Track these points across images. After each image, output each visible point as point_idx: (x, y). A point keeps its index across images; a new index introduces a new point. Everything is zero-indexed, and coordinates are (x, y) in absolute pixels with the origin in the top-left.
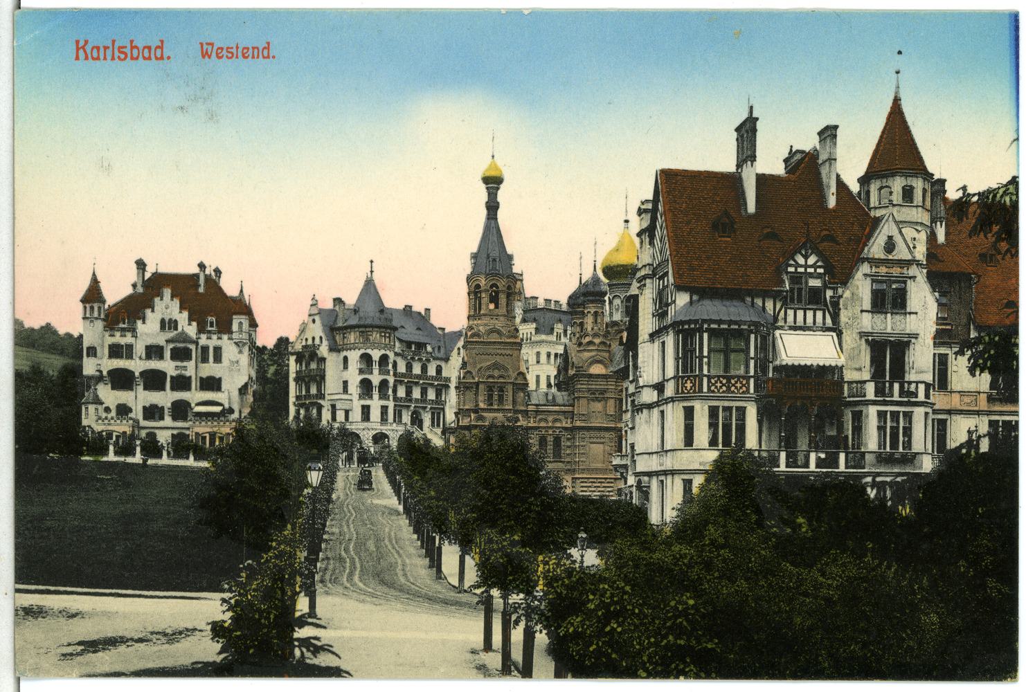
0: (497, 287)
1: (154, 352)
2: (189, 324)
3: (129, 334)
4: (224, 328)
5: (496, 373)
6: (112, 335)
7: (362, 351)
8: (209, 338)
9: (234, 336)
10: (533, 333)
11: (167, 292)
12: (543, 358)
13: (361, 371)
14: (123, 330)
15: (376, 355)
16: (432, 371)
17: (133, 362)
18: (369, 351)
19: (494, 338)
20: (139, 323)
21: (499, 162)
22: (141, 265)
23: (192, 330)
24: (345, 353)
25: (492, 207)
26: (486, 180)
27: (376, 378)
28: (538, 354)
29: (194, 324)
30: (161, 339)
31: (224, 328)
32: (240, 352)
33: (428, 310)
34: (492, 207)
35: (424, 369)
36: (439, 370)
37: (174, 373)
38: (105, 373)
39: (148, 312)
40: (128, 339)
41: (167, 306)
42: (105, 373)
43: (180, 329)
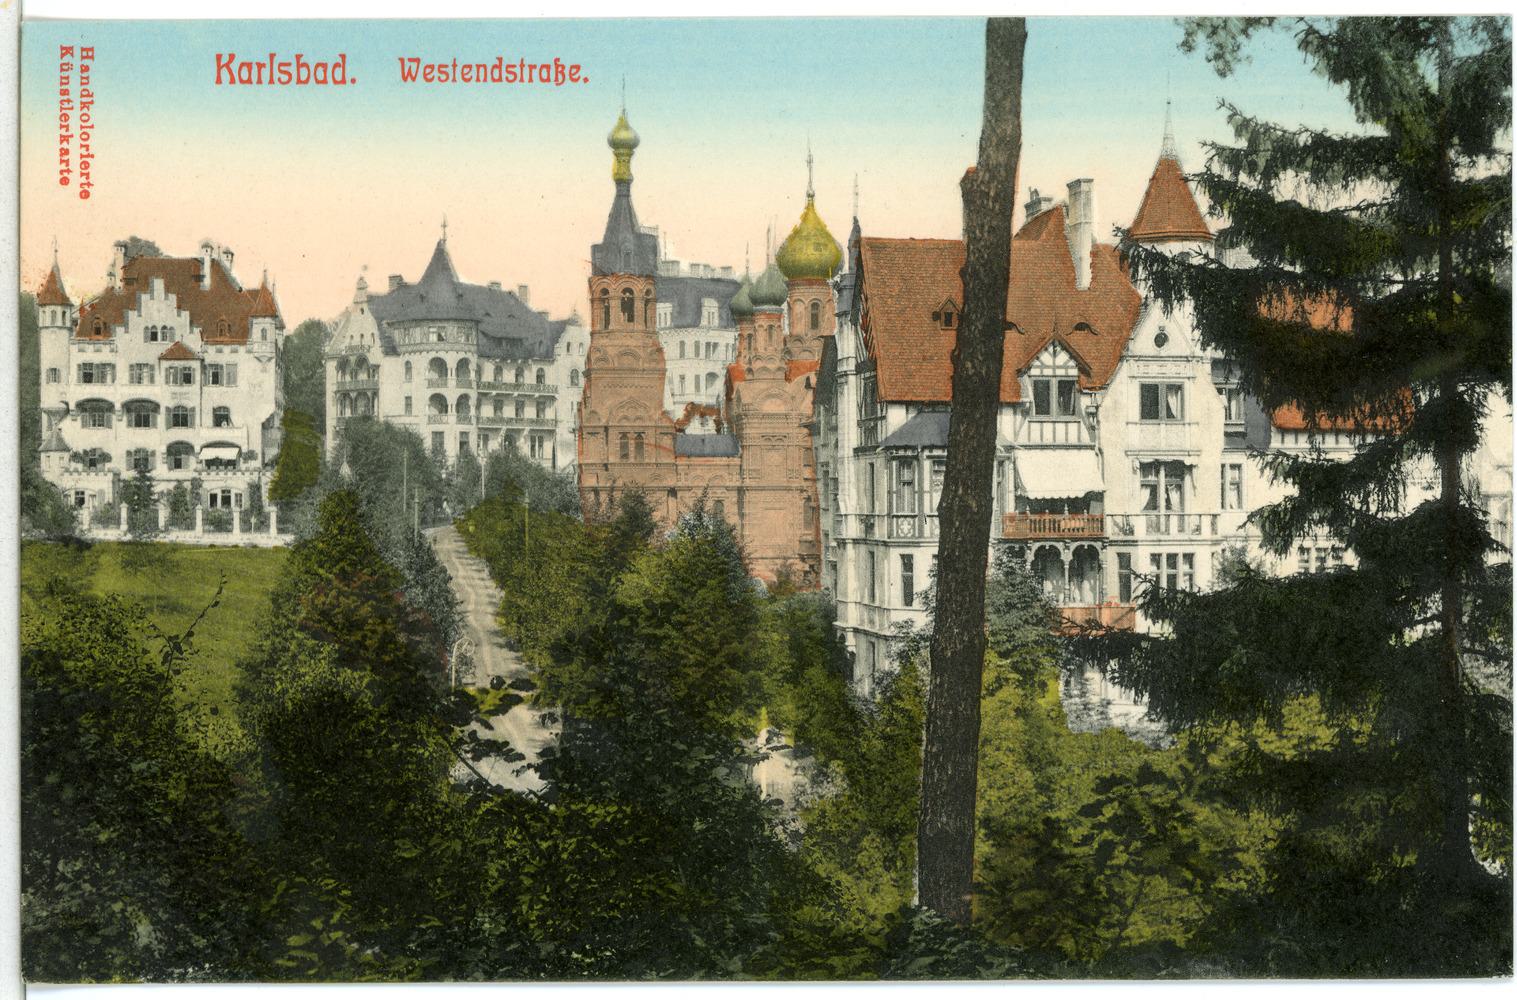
0: (631, 291)
1: (138, 372)
2: (191, 332)
3: (106, 349)
4: (241, 336)
5: (631, 413)
7: (433, 355)
8: (220, 351)
11: (159, 284)
12: (690, 350)
13: (431, 384)
15: (452, 360)
16: (529, 377)
17: (111, 389)
18: (442, 355)
20: (120, 330)
23: (193, 341)
24: (407, 357)
27: (452, 394)
31: (241, 336)
32: (264, 370)
33: (523, 288)
36: (540, 377)
37: (171, 405)
38: (72, 406)
39: (132, 315)
41: (158, 306)
42: (72, 406)
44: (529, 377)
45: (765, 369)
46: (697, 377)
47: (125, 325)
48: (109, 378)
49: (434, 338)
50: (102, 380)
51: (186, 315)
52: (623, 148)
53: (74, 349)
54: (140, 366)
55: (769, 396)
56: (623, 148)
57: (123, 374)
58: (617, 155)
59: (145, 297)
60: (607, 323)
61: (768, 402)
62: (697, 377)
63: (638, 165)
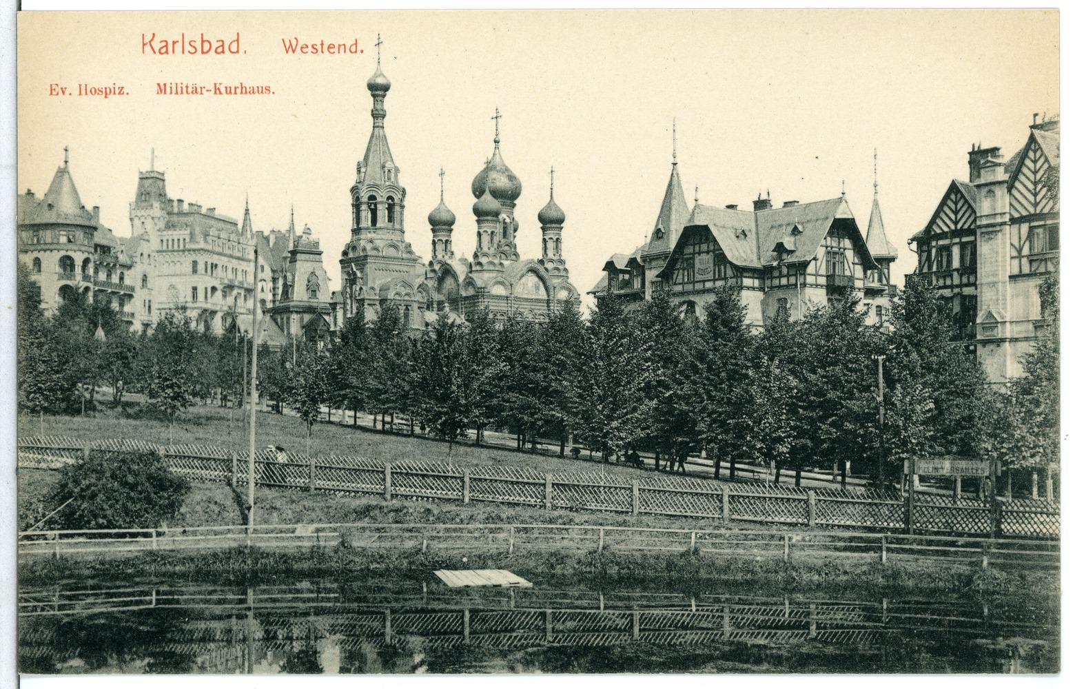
7: (63, 253)
10: (187, 240)
12: (201, 267)
13: (61, 278)
15: (79, 258)
16: (115, 279)
18: (70, 253)
21: (385, 69)
24: (36, 254)
25: (378, 115)
26: (373, 87)
28: (195, 263)
33: (96, 208)
34: (378, 115)
35: (109, 275)
36: (122, 279)
44: (115, 279)
45: (491, 263)
46: (206, 288)
49: (63, 239)
52: (378, 90)
56: (378, 90)
58: (373, 96)
61: (496, 287)
62: (206, 288)
63: (389, 102)
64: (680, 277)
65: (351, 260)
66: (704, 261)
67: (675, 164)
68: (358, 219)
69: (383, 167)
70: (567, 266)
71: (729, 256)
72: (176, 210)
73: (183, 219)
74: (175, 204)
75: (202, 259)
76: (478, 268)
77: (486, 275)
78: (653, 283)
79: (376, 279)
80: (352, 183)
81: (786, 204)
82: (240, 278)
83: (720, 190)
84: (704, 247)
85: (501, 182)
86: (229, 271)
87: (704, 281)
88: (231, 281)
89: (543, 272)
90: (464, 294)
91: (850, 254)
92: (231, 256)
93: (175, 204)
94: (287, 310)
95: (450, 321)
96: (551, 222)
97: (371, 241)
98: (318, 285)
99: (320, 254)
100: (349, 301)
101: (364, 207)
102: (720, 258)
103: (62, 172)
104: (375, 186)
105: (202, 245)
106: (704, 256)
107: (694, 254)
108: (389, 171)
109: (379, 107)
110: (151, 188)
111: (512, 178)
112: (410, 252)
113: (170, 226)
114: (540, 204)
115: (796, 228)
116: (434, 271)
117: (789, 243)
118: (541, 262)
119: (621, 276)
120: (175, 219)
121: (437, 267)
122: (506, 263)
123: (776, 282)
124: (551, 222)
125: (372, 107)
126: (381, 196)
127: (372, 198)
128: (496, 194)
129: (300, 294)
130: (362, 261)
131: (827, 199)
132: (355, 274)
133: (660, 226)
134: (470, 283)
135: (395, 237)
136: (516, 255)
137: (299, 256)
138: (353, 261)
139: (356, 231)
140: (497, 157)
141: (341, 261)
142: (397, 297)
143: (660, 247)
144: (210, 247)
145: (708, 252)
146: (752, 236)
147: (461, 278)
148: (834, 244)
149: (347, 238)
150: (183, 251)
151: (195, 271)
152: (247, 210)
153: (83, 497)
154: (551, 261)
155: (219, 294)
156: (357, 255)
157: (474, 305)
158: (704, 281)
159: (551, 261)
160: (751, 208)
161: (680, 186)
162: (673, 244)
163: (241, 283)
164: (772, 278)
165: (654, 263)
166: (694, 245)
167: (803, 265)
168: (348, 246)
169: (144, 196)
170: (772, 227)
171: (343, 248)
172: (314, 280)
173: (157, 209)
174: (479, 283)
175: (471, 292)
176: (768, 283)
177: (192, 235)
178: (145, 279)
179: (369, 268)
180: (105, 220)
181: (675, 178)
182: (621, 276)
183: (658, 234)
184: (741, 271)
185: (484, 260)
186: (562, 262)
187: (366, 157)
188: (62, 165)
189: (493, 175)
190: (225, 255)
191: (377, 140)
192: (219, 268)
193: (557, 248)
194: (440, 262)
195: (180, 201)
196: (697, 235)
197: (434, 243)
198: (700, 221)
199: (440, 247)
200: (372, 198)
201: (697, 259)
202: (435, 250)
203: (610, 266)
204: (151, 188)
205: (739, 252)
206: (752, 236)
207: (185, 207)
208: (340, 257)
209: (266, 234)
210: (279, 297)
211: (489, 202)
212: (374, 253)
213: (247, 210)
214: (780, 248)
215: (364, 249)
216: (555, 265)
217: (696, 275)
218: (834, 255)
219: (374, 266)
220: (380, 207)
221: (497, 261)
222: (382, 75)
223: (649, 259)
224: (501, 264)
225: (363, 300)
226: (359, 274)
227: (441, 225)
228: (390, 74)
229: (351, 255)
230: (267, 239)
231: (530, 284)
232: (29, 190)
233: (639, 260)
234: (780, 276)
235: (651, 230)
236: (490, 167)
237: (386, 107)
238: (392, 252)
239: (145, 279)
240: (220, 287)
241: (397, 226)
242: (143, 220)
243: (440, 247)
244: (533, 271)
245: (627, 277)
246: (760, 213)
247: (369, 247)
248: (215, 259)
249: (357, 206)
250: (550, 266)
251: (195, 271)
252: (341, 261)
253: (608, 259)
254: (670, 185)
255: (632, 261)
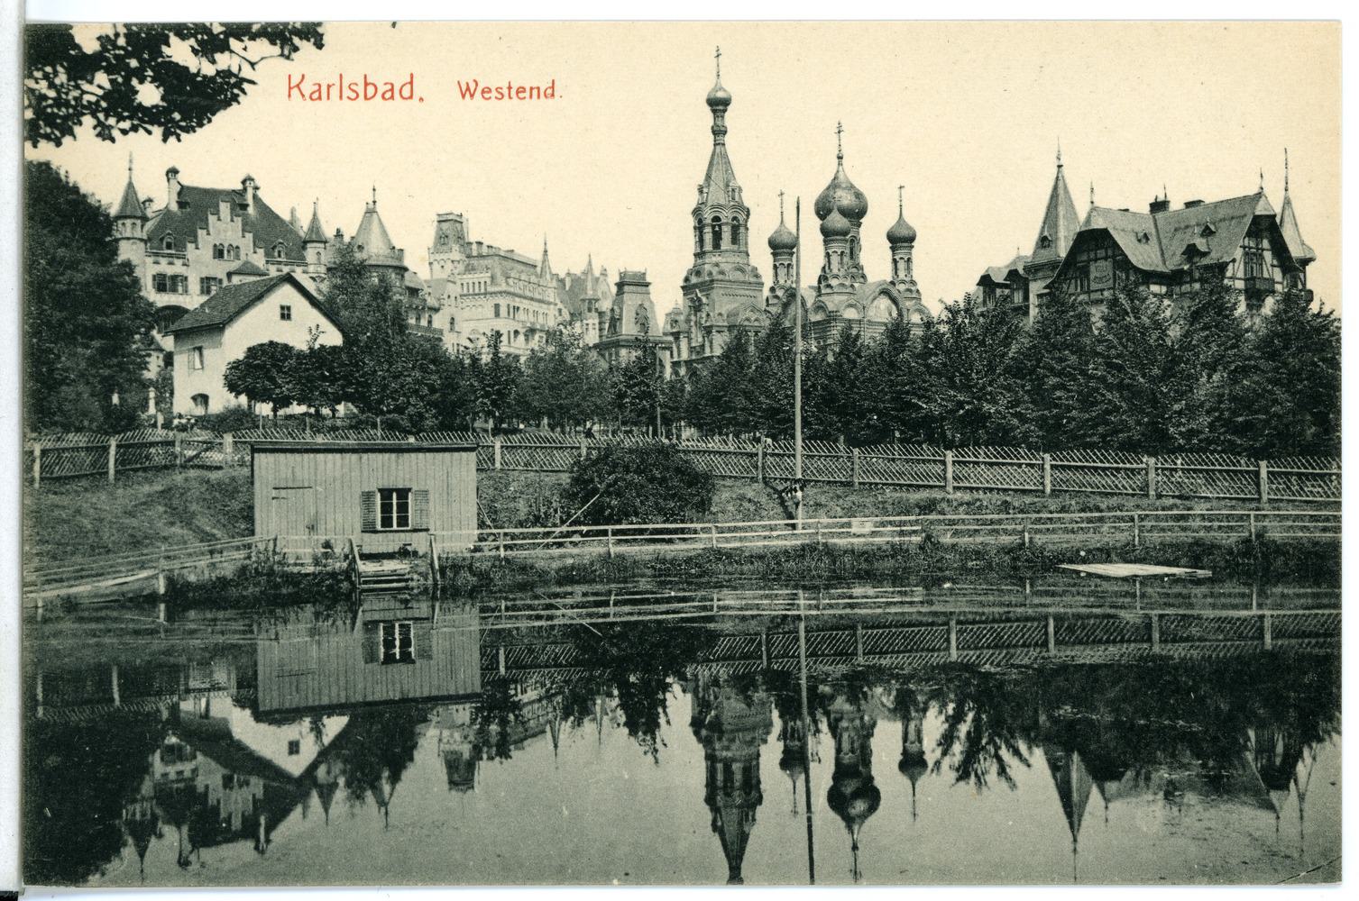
3: (178, 262)
6: (156, 263)
9: (311, 269)
10: (489, 281)
11: (225, 208)
12: (503, 311)
14: (170, 256)
16: (424, 323)
17: (188, 299)
19: (739, 276)
20: (190, 246)
22: (173, 172)
23: (259, 259)
25: (719, 132)
28: (497, 306)
29: (261, 252)
30: (219, 269)
34: (719, 132)
35: (418, 319)
36: (430, 322)
40: (177, 268)
41: (224, 228)
43: (243, 257)
44: (424, 323)
45: (842, 285)
47: (195, 241)
48: (180, 289)
50: (174, 290)
51: (249, 236)
52: (718, 105)
53: (150, 260)
54: (208, 279)
55: (851, 306)
56: (718, 105)
57: (194, 286)
59: (212, 219)
60: (702, 247)
63: (730, 118)
64: (1072, 286)
65: (695, 286)
66: (1100, 269)
67: (1060, 166)
68: (701, 241)
69: (728, 186)
70: (919, 287)
71: (1134, 261)
72: (475, 253)
73: (484, 262)
74: (474, 247)
75: (503, 302)
76: (829, 291)
77: (837, 298)
78: (1040, 296)
79: (722, 306)
80: (694, 206)
81: (1189, 205)
82: (541, 320)
83: (1116, 189)
84: (1101, 253)
85: (846, 199)
86: (531, 315)
87: (1102, 290)
88: (533, 324)
89: (895, 293)
90: (813, 320)
91: (1268, 255)
92: (532, 299)
93: (474, 247)
94: (617, 345)
95: (854, 333)
96: (901, 241)
97: (717, 265)
98: (646, 318)
99: (647, 285)
100: (693, 329)
101: (708, 230)
102: (1123, 263)
103: (370, 212)
104: (719, 206)
105: (504, 287)
106: (1102, 263)
107: (1089, 261)
108: (732, 191)
109: (719, 123)
110: (450, 231)
111: (858, 195)
112: (757, 276)
113: (470, 269)
114: (890, 222)
115: (1207, 227)
116: (777, 297)
117: (1201, 244)
118: (893, 283)
119: (998, 291)
120: (474, 262)
121: (780, 293)
122: (856, 285)
123: (1186, 288)
124: (901, 241)
125: (712, 123)
126: (726, 216)
127: (716, 219)
128: (845, 212)
129: (628, 329)
130: (707, 286)
131: (1241, 195)
132: (699, 300)
133: (1046, 234)
134: (820, 307)
135: (740, 260)
136: (864, 276)
137: (626, 288)
138: (696, 287)
139: (700, 255)
140: (841, 173)
141: (683, 288)
142: (746, 323)
143: (1046, 255)
144: (512, 290)
145: (1106, 258)
146: (1153, 240)
147: (809, 304)
148: (1252, 244)
149: (689, 262)
150: (485, 294)
151: (497, 314)
152: (546, 251)
153: (609, 494)
154: (903, 282)
155: (521, 338)
156: (700, 280)
157: (825, 330)
158: (1102, 290)
159: (903, 282)
160: (1146, 210)
161: (1065, 187)
162: (1063, 254)
163: (543, 326)
164: (1181, 284)
165: (1040, 274)
166: (1089, 251)
167: (1222, 267)
168: (690, 272)
169: (442, 240)
170: (1176, 230)
171: (684, 274)
172: (642, 312)
173: (456, 254)
174: (831, 307)
175: (819, 317)
176: (1177, 289)
177: (493, 278)
178: (452, 321)
179: (715, 294)
180: (408, 262)
181: (1061, 184)
182: (998, 291)
183: (1044, 242)
184: (1149, 277)
185: (834, 282)
186: (913, 283)
187: (708, 177)
188: (371, 206)
189: (839, 193)
190: (525, 298)
191: (719, 160)
192: (521, 311)
193: (909, 269)
194: (782, 288)
195: (480, 243)
196: (1094, 241)
197: (775, 267)
198: (1098, 223)
199: (782, 272)
200: (716, 219)
201: (1092, 268)
202: (776, 275)
203: (986, 281)
204: (450, 231)
205: (1143, 256)
206: (1153, 240)
207: (485, 251)
208: (682, 283)
209: (562, 275)
210: (606, 332)
211: (837, 221)
212: (720, 277)
213: (546, 251)
214: (1191, 252)
215: (710, 274)
216: (907, 286)
217: (1092, 284)
218: (1253, 257)
219: (722, 292)
220: (725, 228)
221: (848, 283)
222: (721, 89)
223: (1034, 269)
224: (852, 286)
225: (711, 327)
226: (704, 300)
227: (783, 248)
228: (731, 87)
229: (694, 280)
230: (562, 281)
231: (882, 307)
232: (338, 231)
233: (1021, 272)
234: (1193, 280)
235: (1035, 236)
236: (834, 185)
237: (726, 124)
238: (739, 276)
239: (452, 321)
240: (522, 331)
241: (742, 249)
242: (442, 263)
243: (782, 272)
244: (885, 292)
245: (1007, 291)
246: (1160, 215)
247: (715, 271)
248: (517, 302)
249: (699, 229)
250: (902, 287)
251: (497, 314)
252: (683, 288)
253: (982, 273)
254: (1055, 188)
255: (1013, 274)
